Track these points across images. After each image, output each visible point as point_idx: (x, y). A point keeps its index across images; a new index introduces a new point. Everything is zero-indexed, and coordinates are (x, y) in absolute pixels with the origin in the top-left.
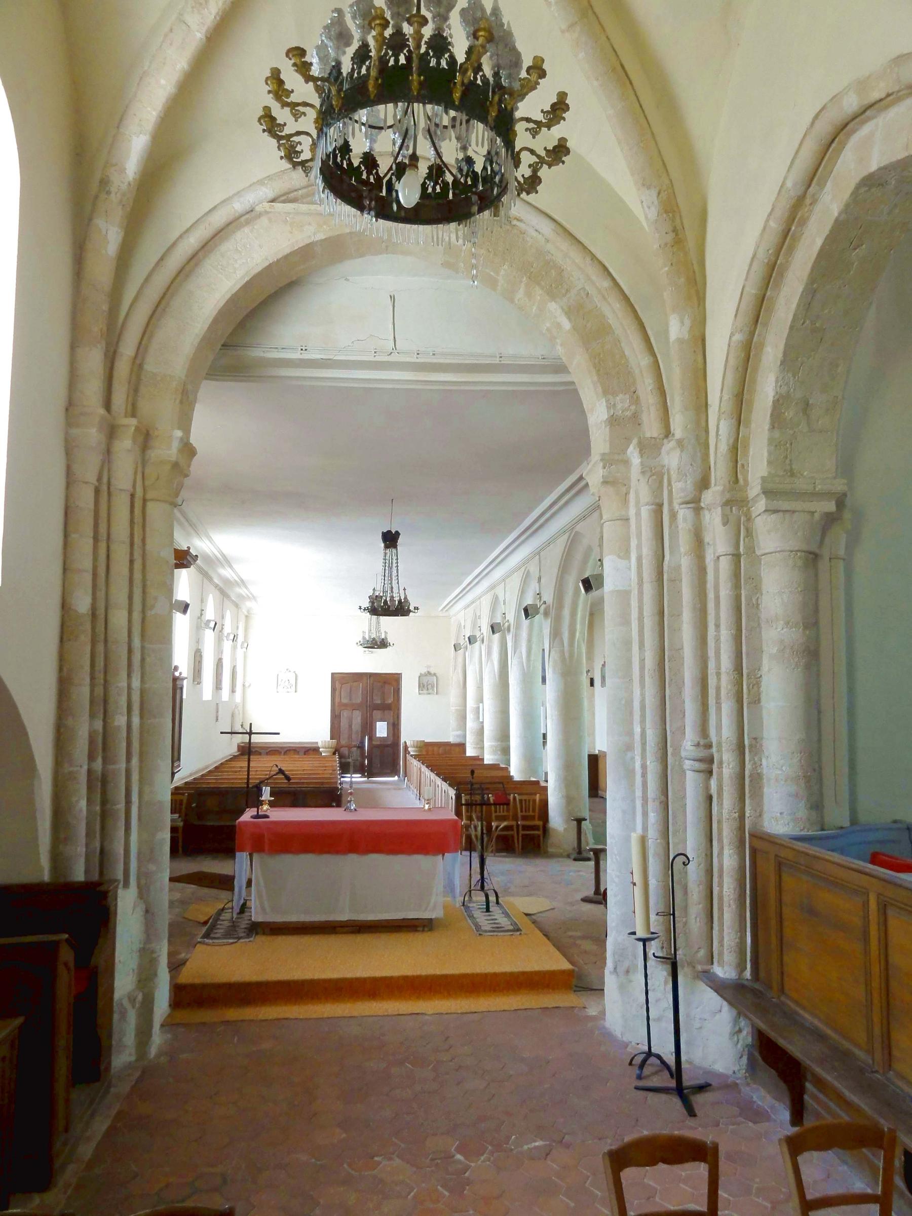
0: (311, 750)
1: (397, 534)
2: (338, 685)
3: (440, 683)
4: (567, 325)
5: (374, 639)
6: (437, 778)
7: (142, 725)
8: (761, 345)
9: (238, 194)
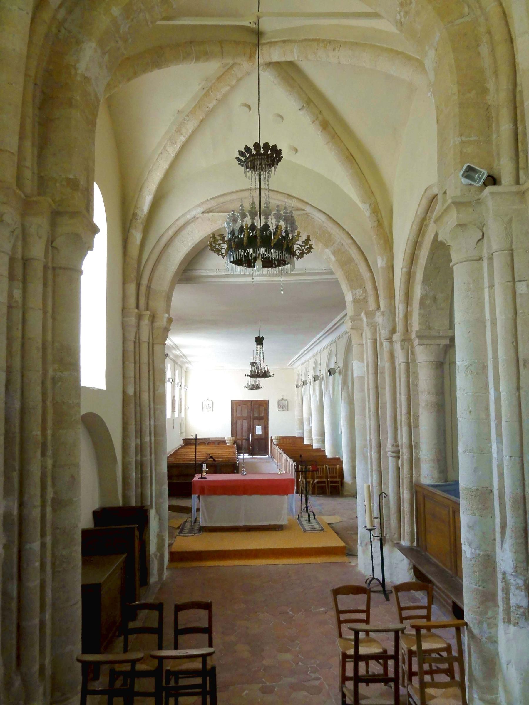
0: (221, 442)
1: (263, 338)
4: (333, 259)
5: (253, 385)
7: (155, 440)
8: (415, 273)
9: (189, 211)
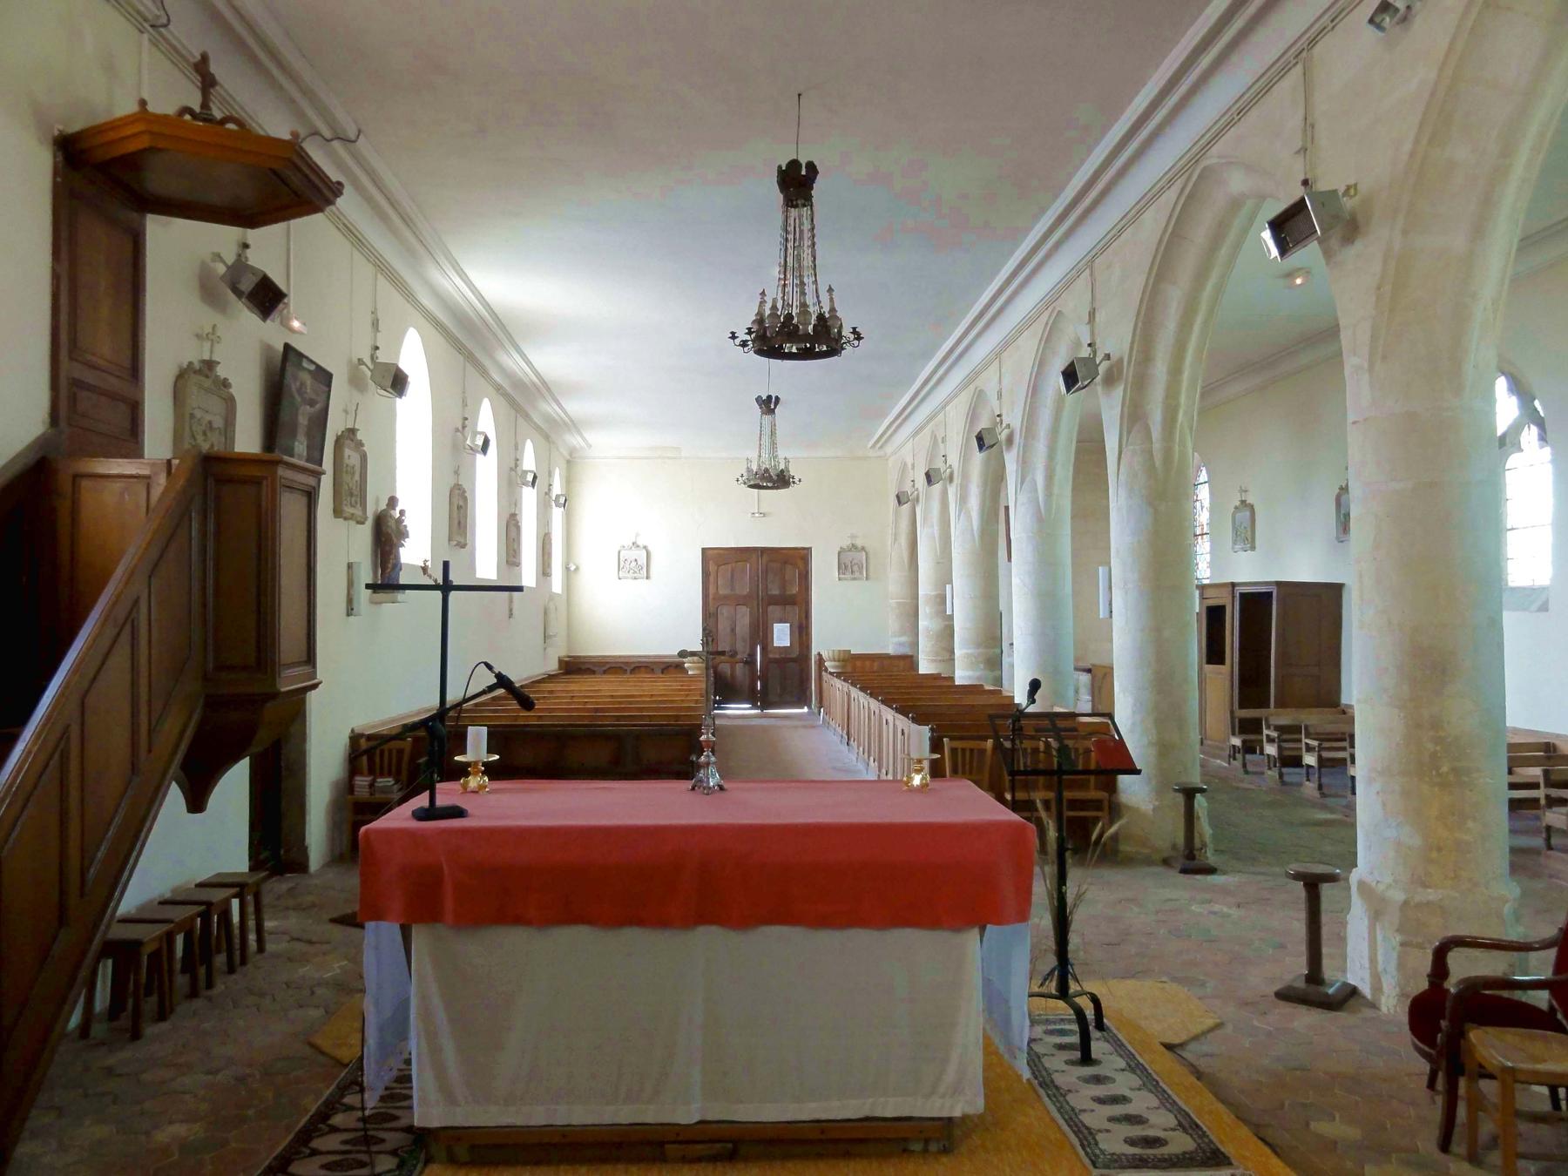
2: (712, 568)
3: (872, 561)
5: (766, 470)
6: (883, 707)
